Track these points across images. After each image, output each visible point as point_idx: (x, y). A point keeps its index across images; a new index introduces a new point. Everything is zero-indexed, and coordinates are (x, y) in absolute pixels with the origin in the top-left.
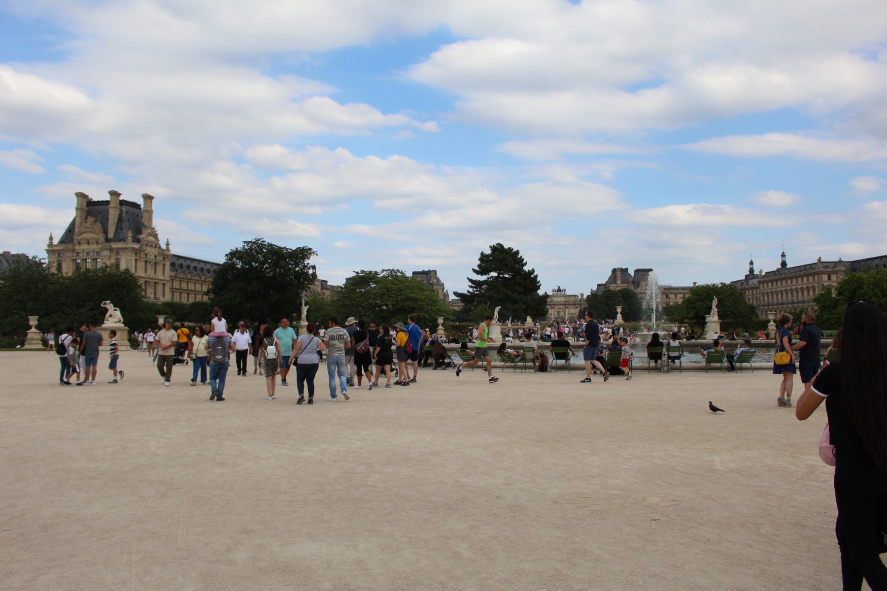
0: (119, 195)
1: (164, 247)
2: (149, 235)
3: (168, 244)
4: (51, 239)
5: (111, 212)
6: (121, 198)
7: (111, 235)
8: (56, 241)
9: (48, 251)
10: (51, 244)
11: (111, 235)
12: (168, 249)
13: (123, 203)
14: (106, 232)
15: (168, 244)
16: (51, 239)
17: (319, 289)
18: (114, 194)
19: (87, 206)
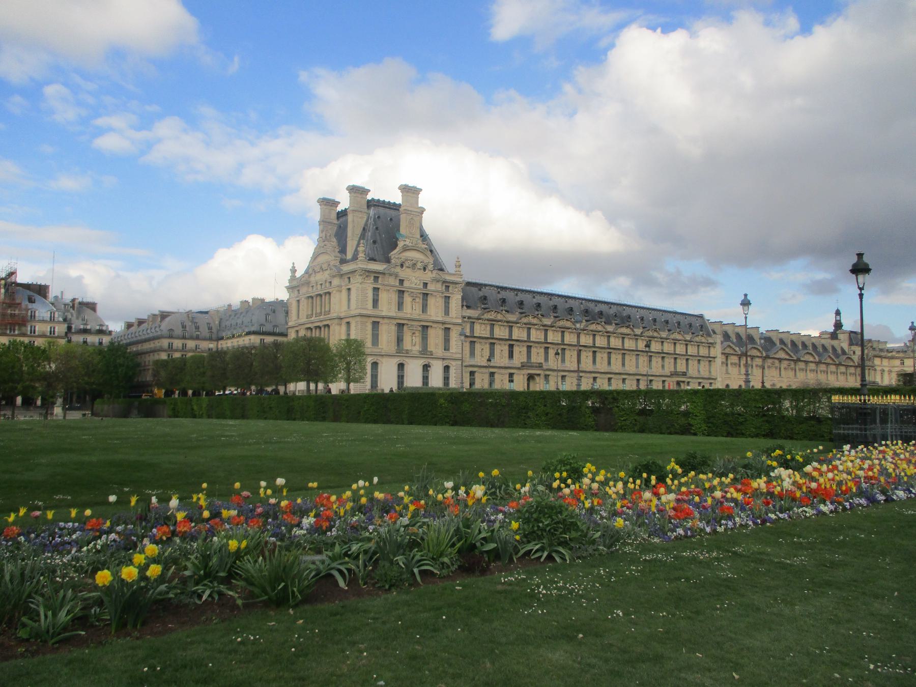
0: (365, 191)
2: (406, 249)
4: (294, 271)
5: (350, 218)
6: (369, 197)
7: (349, 256)
8: (298, 274)
9: (288, 288)
10: (293, 278)
11: (349, 256)
13: (371, 204)
14: (343, 251)
16: (294, 271)
17: (845, 346)
18: (356, 191)
19: (338, 218)
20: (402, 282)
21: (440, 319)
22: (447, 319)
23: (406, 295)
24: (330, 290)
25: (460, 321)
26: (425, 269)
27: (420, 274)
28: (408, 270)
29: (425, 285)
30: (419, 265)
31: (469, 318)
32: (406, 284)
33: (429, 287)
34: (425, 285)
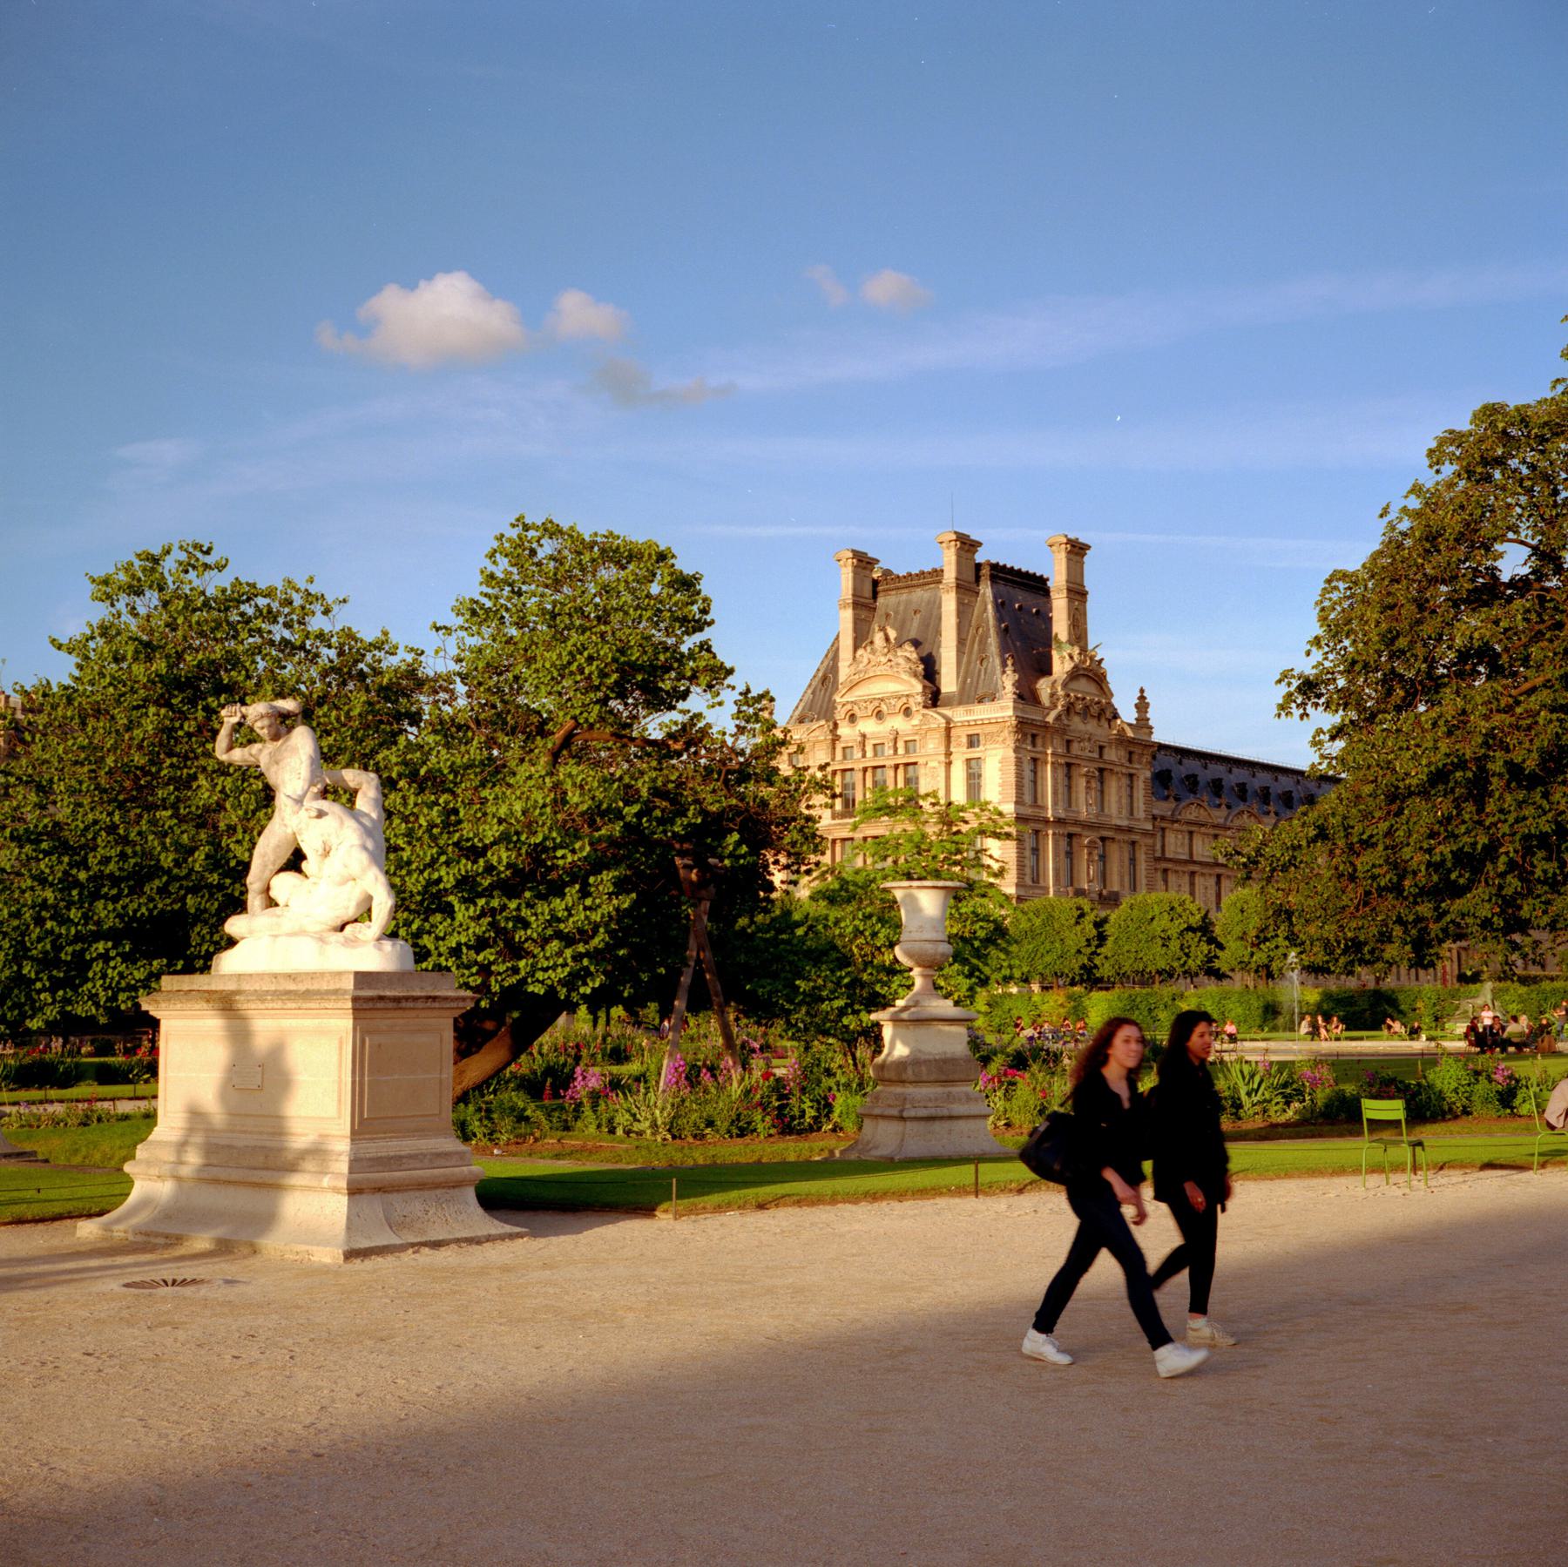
1: (1128, 714)
3: (1142, 705)
6: (980, 557)
11: (949, 682)
12: (1143, 723)
14: (930, 671)
15: (1142, 705)
20: (1069, 742)
21: (1125, 823)
22: (1133, 824)
23: (1075, 772)
24: (921, 761)
25: (1149, 826)
26: (1099, 718)
27: (1091, 727)
28: (1076, 719)
29: (1101, 748)
30: (1095, 710)
31: (1163, 818)
32: (1075, 748)
33: (1112, 755)
34: (1101, 748)
